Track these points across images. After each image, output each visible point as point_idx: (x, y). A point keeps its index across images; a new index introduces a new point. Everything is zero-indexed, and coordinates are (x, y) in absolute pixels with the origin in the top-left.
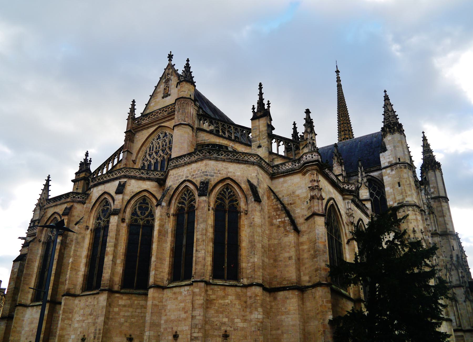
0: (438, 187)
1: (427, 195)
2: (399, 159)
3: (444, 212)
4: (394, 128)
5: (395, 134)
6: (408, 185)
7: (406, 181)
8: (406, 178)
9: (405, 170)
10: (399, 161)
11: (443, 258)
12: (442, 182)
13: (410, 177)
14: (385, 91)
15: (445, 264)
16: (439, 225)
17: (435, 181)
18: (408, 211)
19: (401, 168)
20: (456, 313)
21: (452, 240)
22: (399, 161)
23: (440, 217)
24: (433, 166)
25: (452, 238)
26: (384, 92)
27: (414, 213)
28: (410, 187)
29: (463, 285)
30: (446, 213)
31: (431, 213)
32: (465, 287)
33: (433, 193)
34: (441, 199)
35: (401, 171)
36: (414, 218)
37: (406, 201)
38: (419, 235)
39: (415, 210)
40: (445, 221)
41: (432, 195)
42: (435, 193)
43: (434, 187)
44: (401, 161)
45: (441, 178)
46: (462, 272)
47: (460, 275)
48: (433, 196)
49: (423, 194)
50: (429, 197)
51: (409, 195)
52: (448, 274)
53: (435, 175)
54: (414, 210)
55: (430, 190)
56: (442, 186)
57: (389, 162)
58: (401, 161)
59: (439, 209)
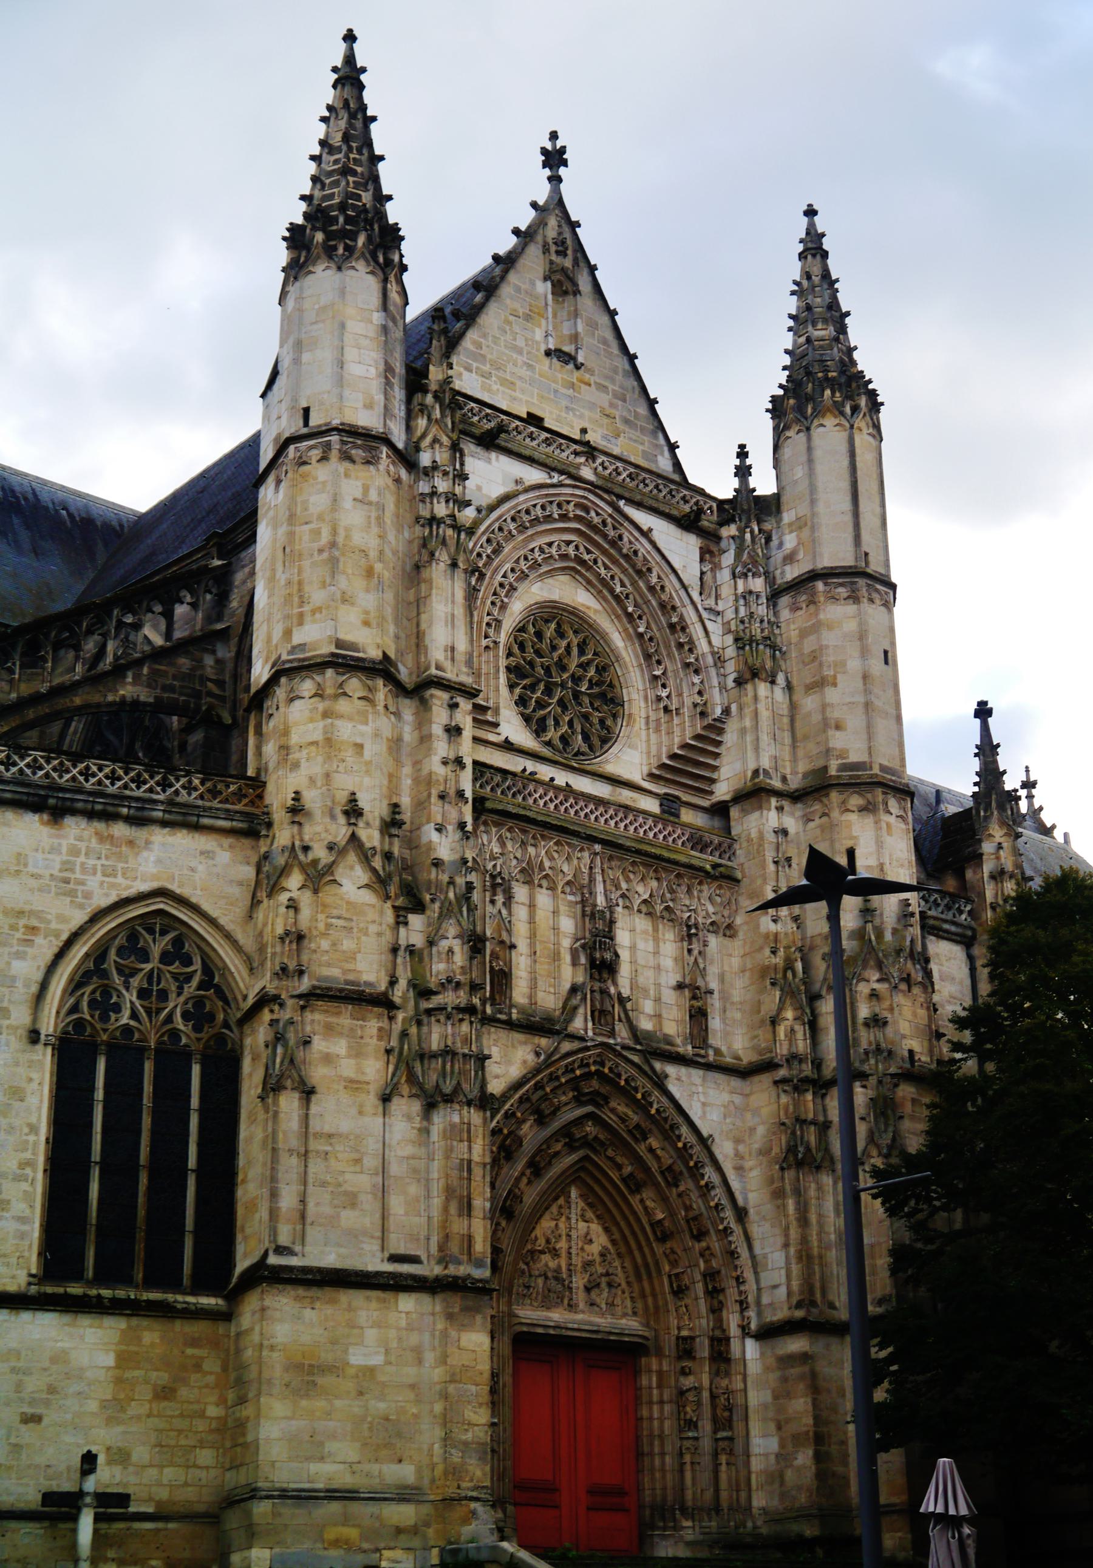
0: (814, 514)
1: (745, 576)
2: (306, 411)
3: (829, 658)
4: (355, 240)
5: (311, 272)
6: (321, 551)
7: (317, 533)
8: (320, 518)
9: (322, 473)
10: (306, 423)
11: (773, 927)
12: (845, 485)
13: (348, 504)
14: (350, 37)
15: (779, 960)
16: (799, 735)
17: (803, 486)
18: (292, 700)
19: (305, 463)
20: (794, 1233)
21: (853, 817)
22: (306, 423)
23: (810, 688)
24: (809, 398)
25: (855, 801)
26: (345, 38)
27: (321, 706)
28: (333, 562)
29: (866, 1068)
30: (841, 665)
31: (748, 676)
32: (873, 1081)
33: (790, 559)
34: (820, 585)
35: (305, 477)
36: (318, 736)
37: (293, 649)
38: (318, 829)
39: (329, 691)
40: (824, 707)
41: (788, 568)
42: (801, 556)
43: (799, 524)
44: (315, 420)
45: (846, 462)
46: (874, 995)
47: (864, 1011)
48: (791, 573)
49: (724, 576)
50: (758, 584)
51: (313, 612)
52: (789, 1014)
53: (809, 449)
54: (319, 695)
55: (781, 545)
56: (847, 505)
57: (276, 439)
58: (315, 420)
59: (810, 644)
